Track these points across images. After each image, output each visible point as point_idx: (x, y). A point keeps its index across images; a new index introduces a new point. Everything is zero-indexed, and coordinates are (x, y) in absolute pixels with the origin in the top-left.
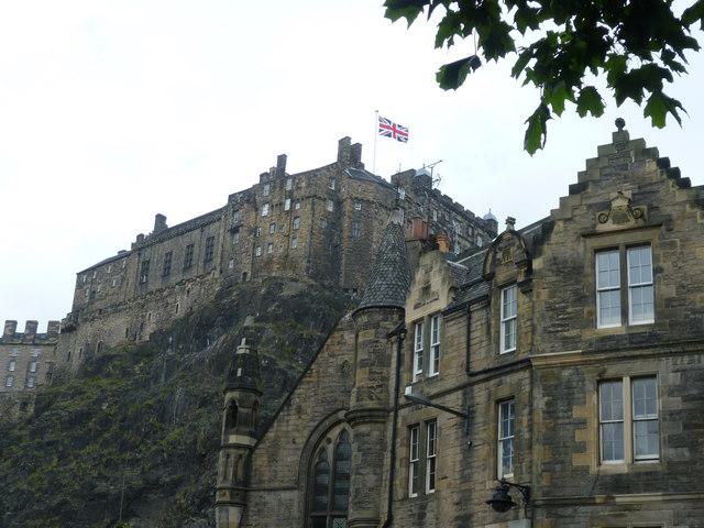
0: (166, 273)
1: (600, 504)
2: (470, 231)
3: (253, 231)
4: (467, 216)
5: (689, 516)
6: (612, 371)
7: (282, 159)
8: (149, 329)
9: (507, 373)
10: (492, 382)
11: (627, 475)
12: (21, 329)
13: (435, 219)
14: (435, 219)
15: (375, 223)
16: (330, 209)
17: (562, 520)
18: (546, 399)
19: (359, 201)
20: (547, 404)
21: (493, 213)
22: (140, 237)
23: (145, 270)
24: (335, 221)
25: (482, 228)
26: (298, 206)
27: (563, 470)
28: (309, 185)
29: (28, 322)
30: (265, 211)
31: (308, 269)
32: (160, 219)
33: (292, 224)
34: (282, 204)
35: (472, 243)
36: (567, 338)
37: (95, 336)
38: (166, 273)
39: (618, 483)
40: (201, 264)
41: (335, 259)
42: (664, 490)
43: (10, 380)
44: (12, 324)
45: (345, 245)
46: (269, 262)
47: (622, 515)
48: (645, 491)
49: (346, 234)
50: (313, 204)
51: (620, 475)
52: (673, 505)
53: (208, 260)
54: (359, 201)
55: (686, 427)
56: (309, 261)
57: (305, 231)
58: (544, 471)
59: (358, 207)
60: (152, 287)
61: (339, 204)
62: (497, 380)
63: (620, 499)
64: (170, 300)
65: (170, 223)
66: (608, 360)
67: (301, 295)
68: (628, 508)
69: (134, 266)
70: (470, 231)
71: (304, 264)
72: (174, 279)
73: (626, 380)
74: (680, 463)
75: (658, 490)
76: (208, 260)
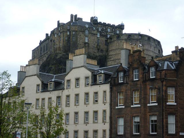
0: (44, 51)
2: (114, 30)
3: (54, 41)
4: (113, 26)
7: (58, 22)
13: (100, 30)
14: (100, 30)
15: (78, 36)
16: (68, 34)
21: (123, 23)
24: (69, 37)
25: (118, 28)
31: (63, 50)
33: (60, 39)
34: (58, 34)
35: (115, 33)
38: (44, 51)
45: (71, 43)
46: (57, 49)
49: (71, 40)
56: (63, 49)
57: (62, 41)
59: (74, 33)
60: (42, 54)
67: (61, 57)
72: (45, 52)
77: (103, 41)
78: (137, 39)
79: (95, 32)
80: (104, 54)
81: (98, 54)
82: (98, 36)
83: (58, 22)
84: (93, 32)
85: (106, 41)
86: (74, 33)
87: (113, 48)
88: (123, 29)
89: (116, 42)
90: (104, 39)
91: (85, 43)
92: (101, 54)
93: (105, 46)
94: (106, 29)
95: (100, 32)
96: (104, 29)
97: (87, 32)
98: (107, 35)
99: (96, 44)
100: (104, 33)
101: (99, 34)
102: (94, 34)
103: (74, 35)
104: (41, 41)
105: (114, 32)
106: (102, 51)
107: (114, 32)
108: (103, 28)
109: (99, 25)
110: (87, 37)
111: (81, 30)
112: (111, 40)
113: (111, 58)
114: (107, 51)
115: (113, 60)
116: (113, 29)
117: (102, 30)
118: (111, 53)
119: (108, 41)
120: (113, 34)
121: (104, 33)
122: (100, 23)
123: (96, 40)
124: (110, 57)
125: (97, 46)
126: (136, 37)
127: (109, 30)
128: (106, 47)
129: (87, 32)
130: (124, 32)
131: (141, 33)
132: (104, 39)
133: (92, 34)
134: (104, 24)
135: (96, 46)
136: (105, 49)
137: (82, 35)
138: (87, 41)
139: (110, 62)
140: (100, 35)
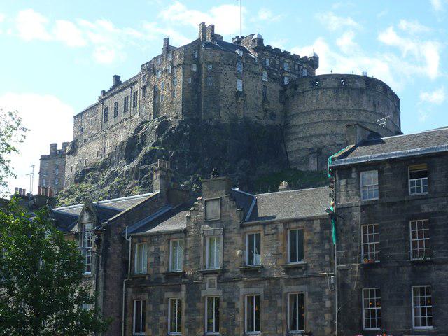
0: (116, 114)
2: (297, 67)
4: (296, 57)
7: (167, 41)
8: (108, 151)
12: (60, 147)
13: (268, 65)
15: (222, 76)
16: (195, 70)
19: (210, 63)
21: (316, 52)
22: (104, 92)
23: (106, 114)
24: (197, 78)
26: (176, 70)
28: (180, 57)
29: (64, 144)
30: (159, 74)
32: (117, 78)
37: (84, 156)
38: (116, 114)
40: (132, 109)
41: (198, 101)
43: (57, 180)
44: (54, 146)
49: (203, 85)
50: (183, 69)
53: (135, 105)
54: (210, 63)
59: (210, 67)
61: (199, 67)
64: (117, 132)
65: (123, 80)
69: (100, 109)
70: (297, 67)
71: (180, 107)
72: (120, 118)
76: (135, 105)
77: (274, 91)
78: (361, 88)
79: (259, 69)
80: (277, 122)
81: (264, 123)
82: (264, 80)
83: (167, 41)
84: (253, 68)
85: (282, 92)
86: (210, 67)
87: (302, 109)
88: (317, 66)
89: (310, 94)
90: (276, 87)
91: (238, 94)
92: (271, 122)
93: (279, 104)
94: (281, 64)
95: (270, 71)
96: (277, 62)
97: (240, 68)
98: (283, 78)
99: (262, 98)
100: (276, 72)
101: (265, 74)
102: (256, 74)
103: (209, 74)
104: (104, 92)
105: (297, 73)
106: (273, 115)
107: (297, 73)
108: (274, 62)
109: (265, 53)
110: (241, 78)
111: (228, 61)
112: (296, 89)
113: (295, 133)
114: (286, 115)
115: (303, 138)
116: (295, 64)
117: (273, 65)
118: (296, 121)
119: (288, 92)
120: (295, 77)
121: (276, 72)
122: (269, 47)
123: (260, 88)
124: (293, 130)
125: (263, 102)
126: (360, 84)
127: (287, 67)
128: (280, 106)
129: (240, 68)
130: (318, 72)
131: (370, 75)
132: (276, 87)
133: (253, 72)
134: (277, 50)
135: (259, 103)
136: (278, 112)
137: (231, 74)
138: (240, 89)
139: (296, 142)
140: (269, 75)
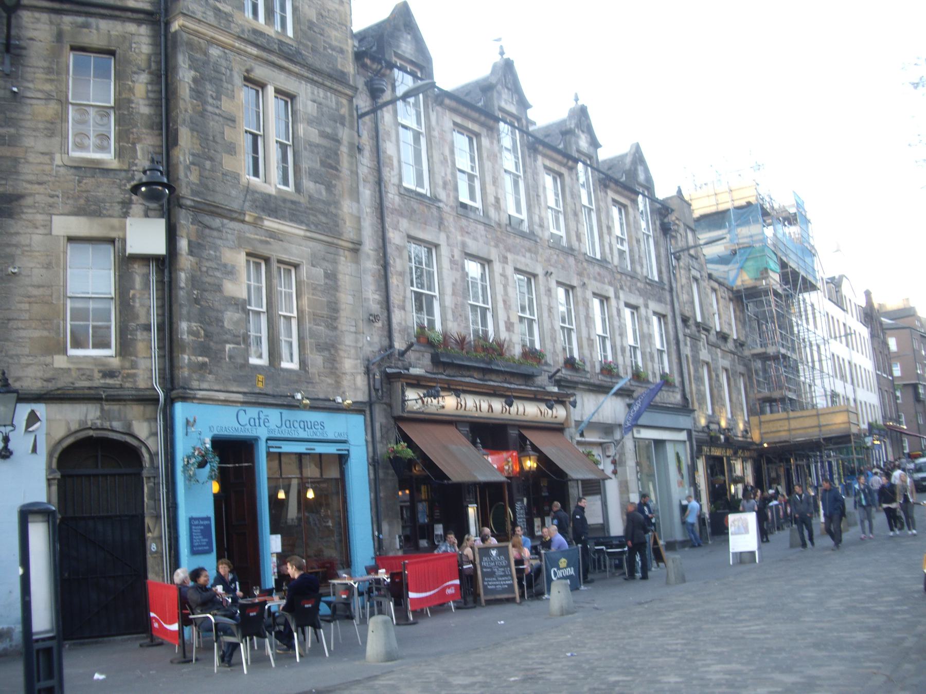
1: (248, 223)
5: (324, 259)
6: (260, 72)
9: (103, 16)
10: (67, 19)
11: (275, 198)
17: (207, 231)
18: (193, 73)
20: (195, 80)
27: (213, 170)
36: (220, 10)
39: (270, 206)
42: (307, 225)
47: (267, 243)
48: (291, 220)
51: (270, 196)
52: (311, 244)
55: (323, 163)
58: (193, 163)
62: (80, 20)
63: (270, 223)
66: (257, 58)
68: (273, 235)
73: (270, 90)
74: (319, 200)
75: (301, 222)
